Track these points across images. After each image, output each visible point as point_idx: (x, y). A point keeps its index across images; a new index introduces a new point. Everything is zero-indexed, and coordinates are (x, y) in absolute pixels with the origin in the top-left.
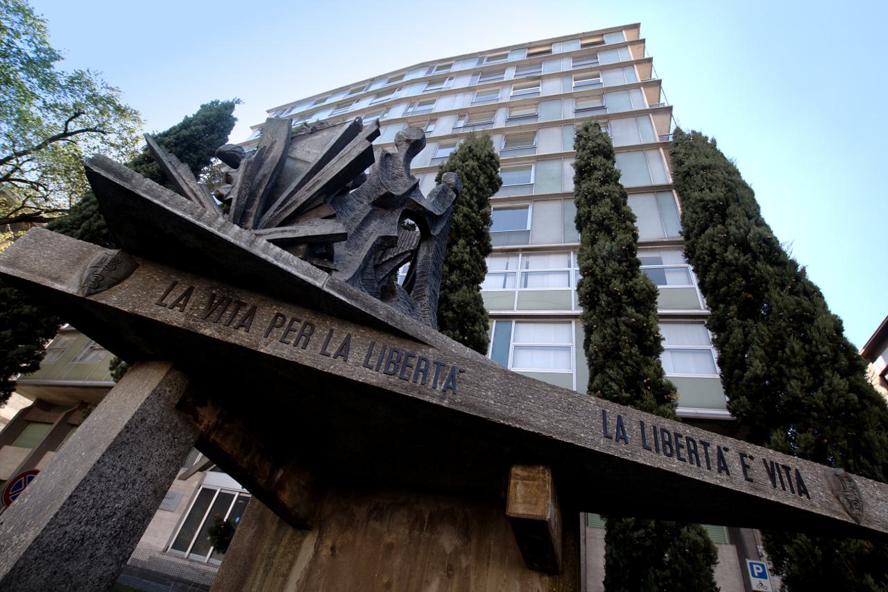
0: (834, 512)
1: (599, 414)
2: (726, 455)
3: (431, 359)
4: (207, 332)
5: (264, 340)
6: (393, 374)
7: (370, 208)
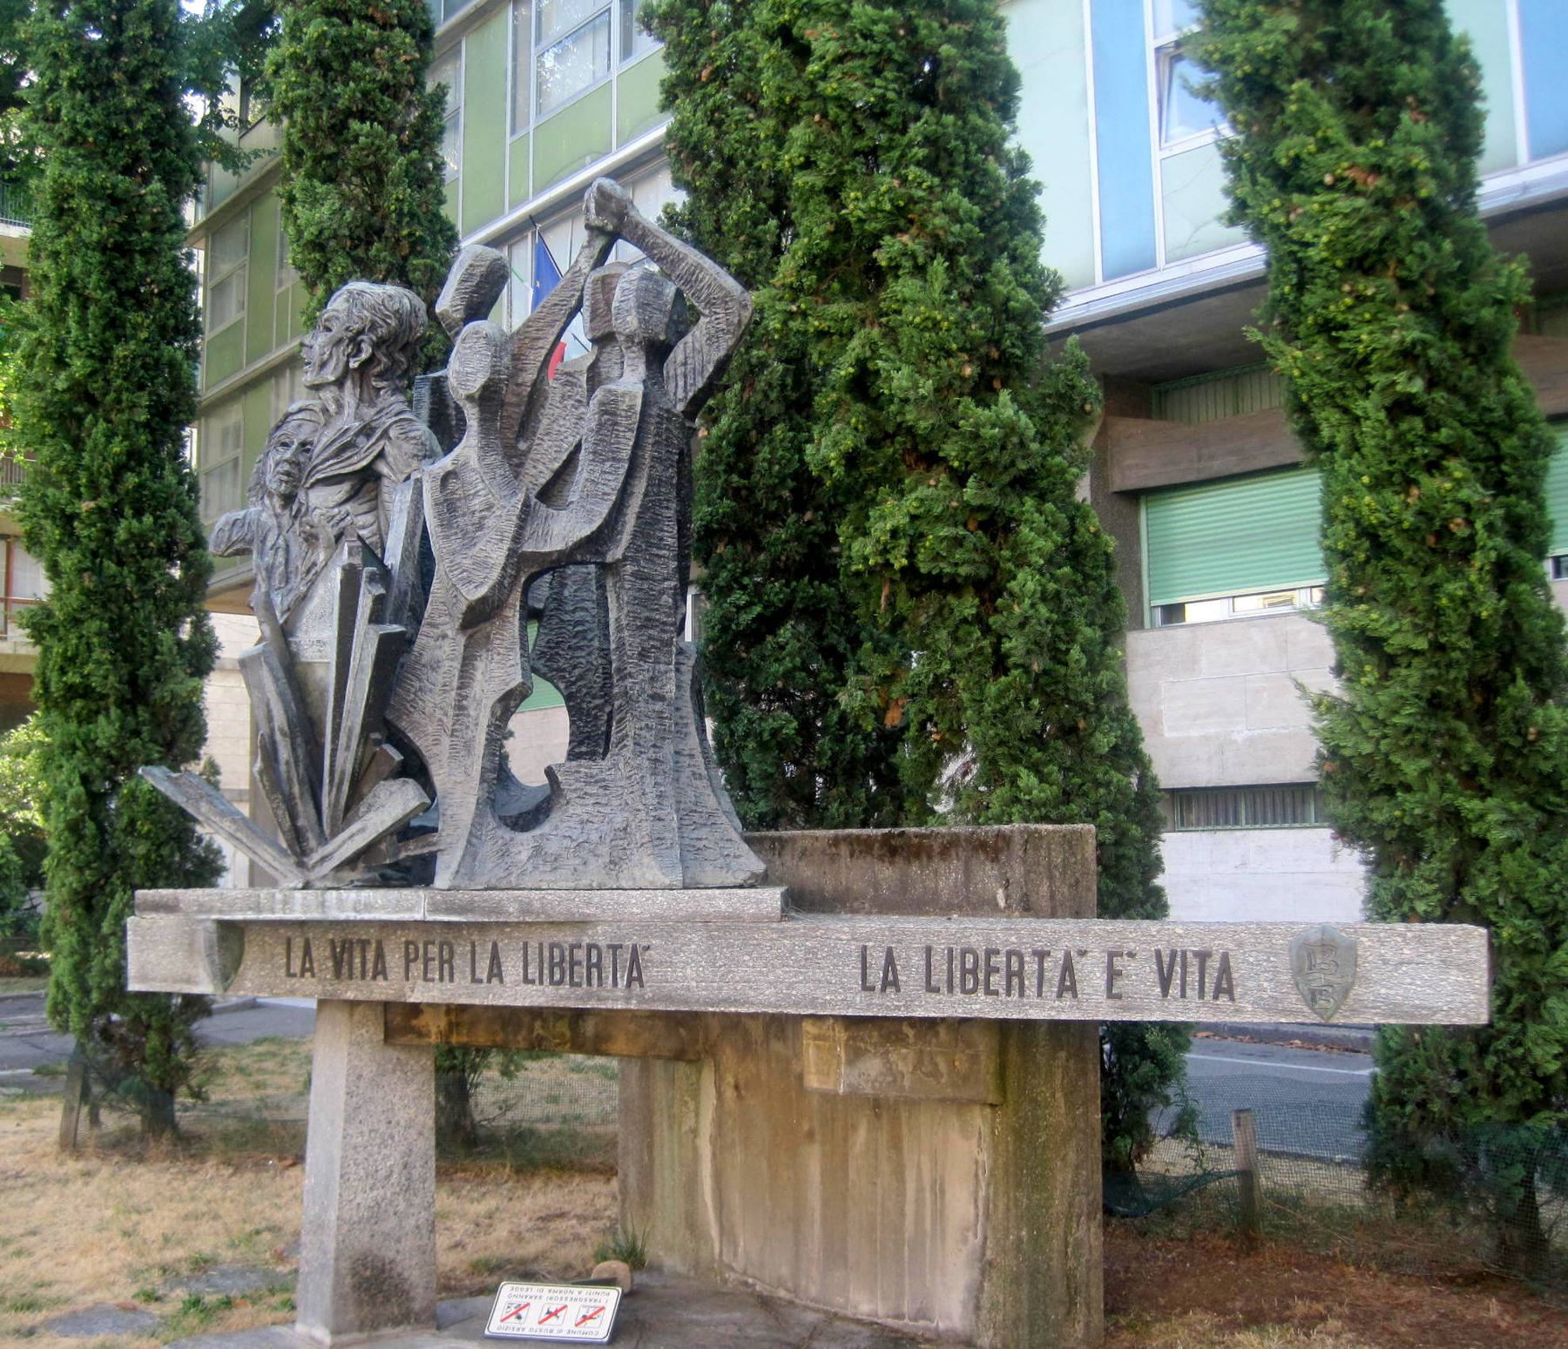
0: (1284, 1012)
1: (856, 955)
2: (1079, 965)
3: (603, 942)
5: (408, 985)
6: (561, 982)
7: (462, 640)
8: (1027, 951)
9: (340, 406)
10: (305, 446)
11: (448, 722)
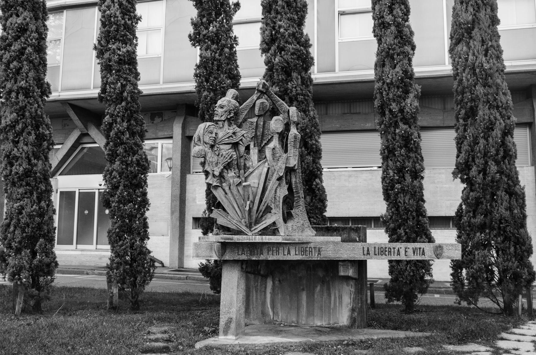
3: (312, 247)
4: (254, 259)
8: (392, 248)
9: (223, 126)
10: (216, 134)
11: (273, 201)
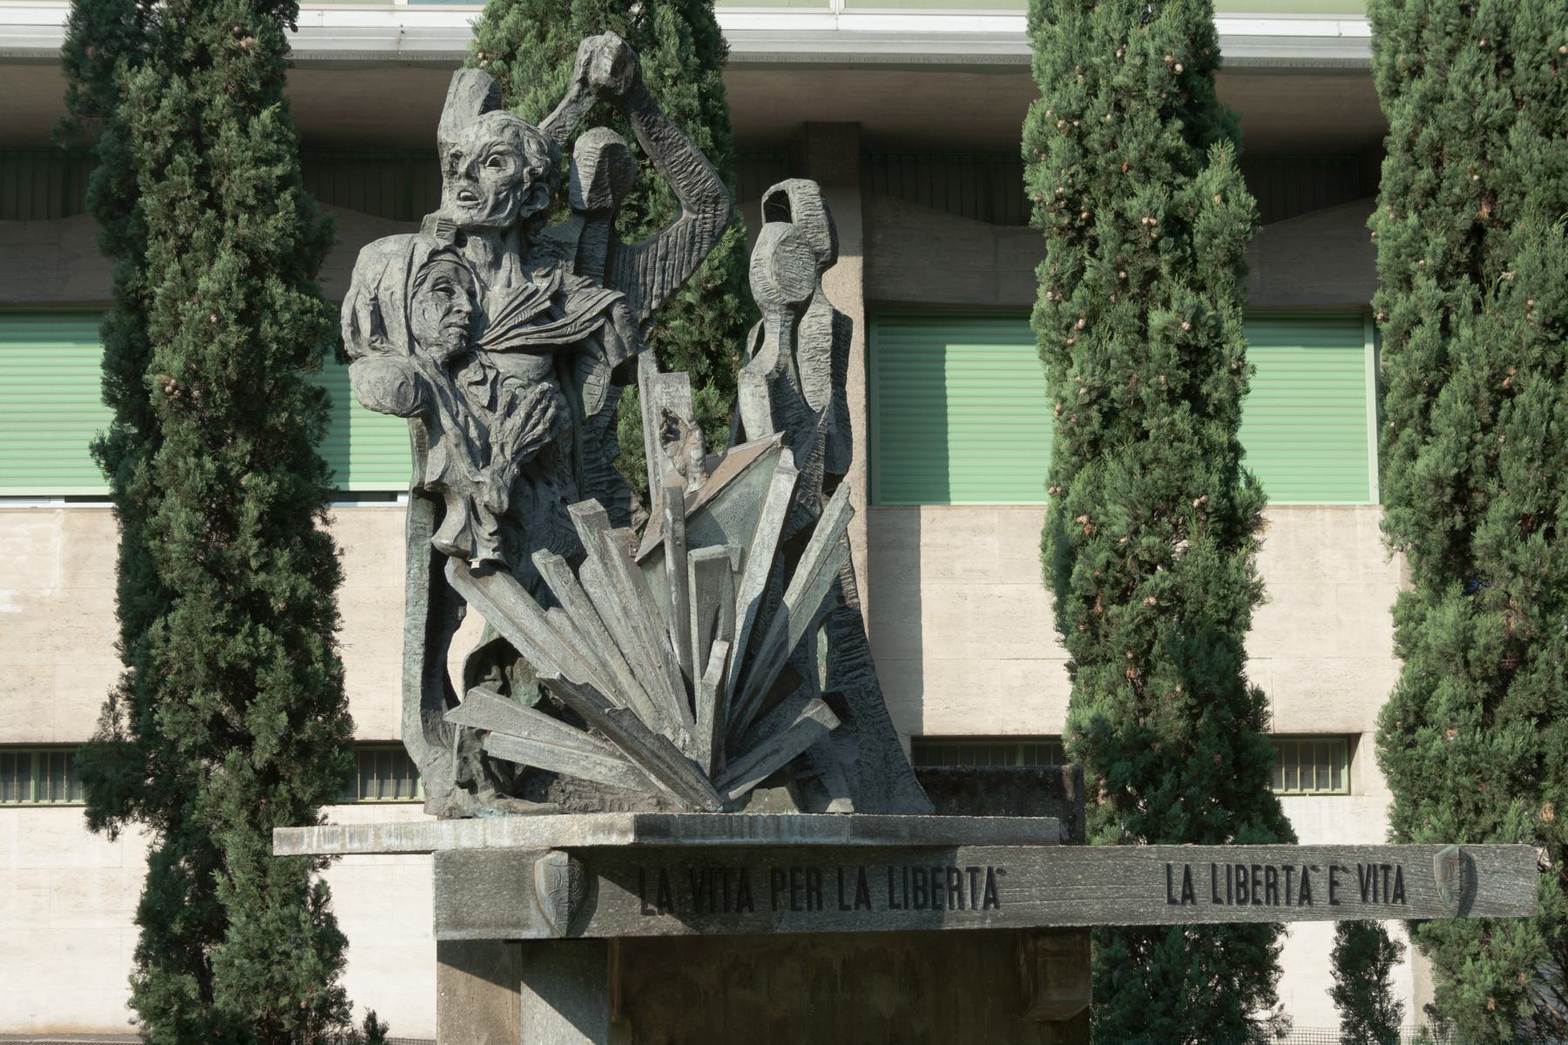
6: (924, 905)
8: (1278, 866)
